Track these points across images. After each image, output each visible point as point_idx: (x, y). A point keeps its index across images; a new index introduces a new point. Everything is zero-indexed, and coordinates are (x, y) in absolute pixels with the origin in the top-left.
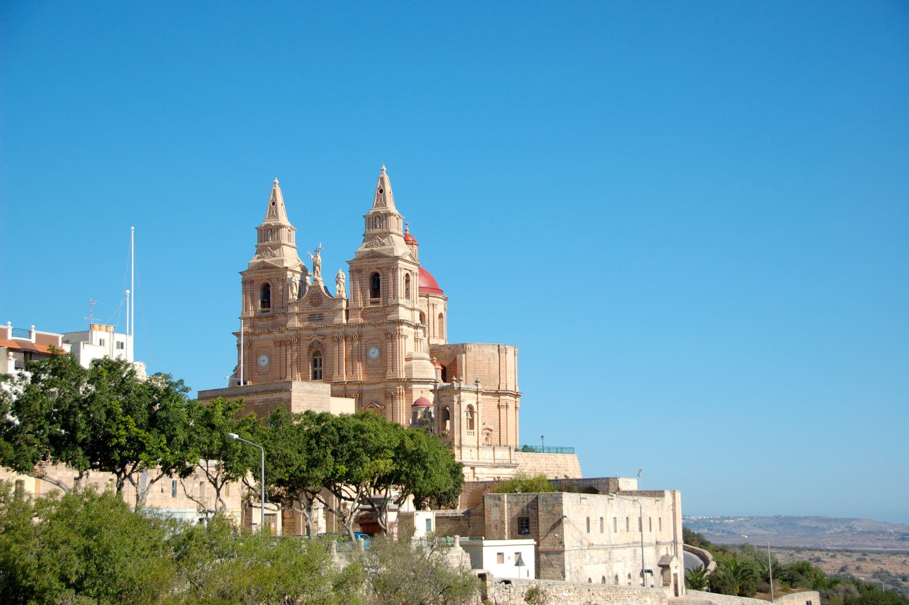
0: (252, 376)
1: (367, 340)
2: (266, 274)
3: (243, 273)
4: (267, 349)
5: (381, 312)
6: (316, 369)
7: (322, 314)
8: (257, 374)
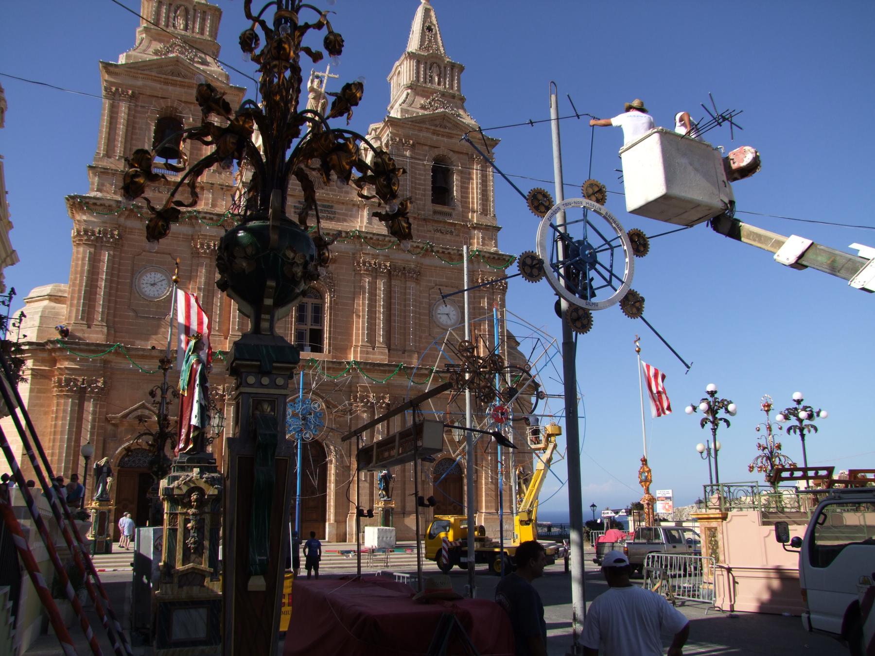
0: (115, 317)
1: (433, 284)
2: (178, 90)
3: (111, 69)
4: (169, 256)
5: (458, 235)
6: (303, 327)
7: (332, 207)
8: (131, 314)
